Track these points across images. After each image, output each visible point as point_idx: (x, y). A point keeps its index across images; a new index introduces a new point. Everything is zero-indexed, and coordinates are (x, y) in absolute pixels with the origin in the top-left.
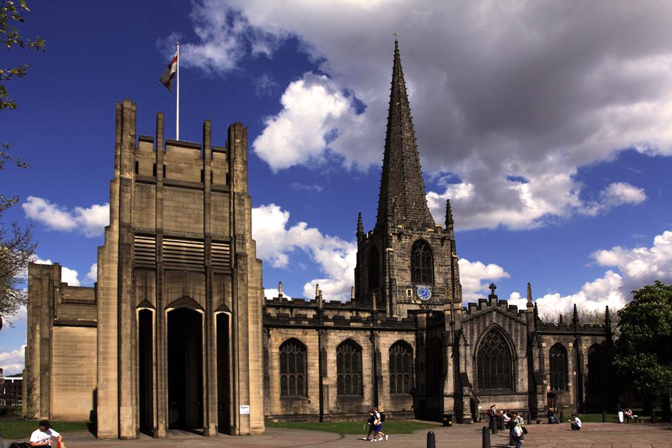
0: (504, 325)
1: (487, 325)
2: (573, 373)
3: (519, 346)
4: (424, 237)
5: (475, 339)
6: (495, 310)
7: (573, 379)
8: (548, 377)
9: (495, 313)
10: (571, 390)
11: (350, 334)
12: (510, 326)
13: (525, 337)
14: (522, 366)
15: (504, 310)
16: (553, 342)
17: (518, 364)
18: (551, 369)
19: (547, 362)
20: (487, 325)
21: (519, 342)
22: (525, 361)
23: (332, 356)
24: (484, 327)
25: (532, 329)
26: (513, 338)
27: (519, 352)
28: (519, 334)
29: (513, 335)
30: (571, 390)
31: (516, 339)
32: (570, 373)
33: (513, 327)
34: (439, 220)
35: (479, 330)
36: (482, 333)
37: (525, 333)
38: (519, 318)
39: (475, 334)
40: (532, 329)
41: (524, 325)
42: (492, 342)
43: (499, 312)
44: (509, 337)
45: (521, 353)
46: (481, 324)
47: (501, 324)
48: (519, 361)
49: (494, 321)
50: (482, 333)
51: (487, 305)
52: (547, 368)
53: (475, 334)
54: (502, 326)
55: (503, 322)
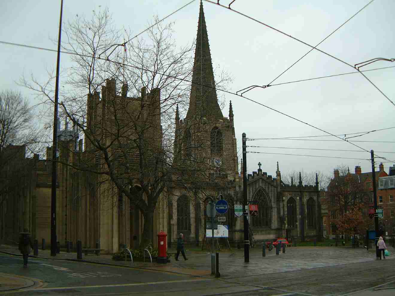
0: (265, 187)
1: (257, 187)
2: (299, 216)
3: (273, 201)
4: (217, 125)
5: (251, 196)
6: (261, 178)
7: (299, 220)
8: (286, 219)
9: (261, 180)
10: (298, 226)
11: (184, 192)
12: (268, 187)
13: (276, 195)
14: (275, 213)
15: (265, 179)
16: (289, 196)
17: (272, 211)
18: (288, 214)
19: (286, 209)
20: (257, 187)
21: (273, 199)
22: (276, 209)
23: (175, 204)
24: (256, 189)
25: (279, 190)
26: (270, 195)
27: (273, 204)
28: (273, 193)
29: (270, 193)
30: (298, 226)
31: (272, 196)
32: (298, 216)
33: (270, 188)
34: (225, 114)
35: (253, 191)
36: (255, 192)
37: (276, 193)
38: (273, 183)
39: (251, 193)
40: (279, 190)
41: (275, 187)
42: (259, 198)
43: (263, 180)
44: (268, 194)
45: (274, 205)
46: (254, 188)
47: (264, 187)
48: (273, 209)
49: (261, 185)
50: (255, 192)
51: (257, 175)
52: (286, 213)
53: (251, 193)
54: (264, 188)
55: (265, 186)
